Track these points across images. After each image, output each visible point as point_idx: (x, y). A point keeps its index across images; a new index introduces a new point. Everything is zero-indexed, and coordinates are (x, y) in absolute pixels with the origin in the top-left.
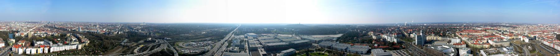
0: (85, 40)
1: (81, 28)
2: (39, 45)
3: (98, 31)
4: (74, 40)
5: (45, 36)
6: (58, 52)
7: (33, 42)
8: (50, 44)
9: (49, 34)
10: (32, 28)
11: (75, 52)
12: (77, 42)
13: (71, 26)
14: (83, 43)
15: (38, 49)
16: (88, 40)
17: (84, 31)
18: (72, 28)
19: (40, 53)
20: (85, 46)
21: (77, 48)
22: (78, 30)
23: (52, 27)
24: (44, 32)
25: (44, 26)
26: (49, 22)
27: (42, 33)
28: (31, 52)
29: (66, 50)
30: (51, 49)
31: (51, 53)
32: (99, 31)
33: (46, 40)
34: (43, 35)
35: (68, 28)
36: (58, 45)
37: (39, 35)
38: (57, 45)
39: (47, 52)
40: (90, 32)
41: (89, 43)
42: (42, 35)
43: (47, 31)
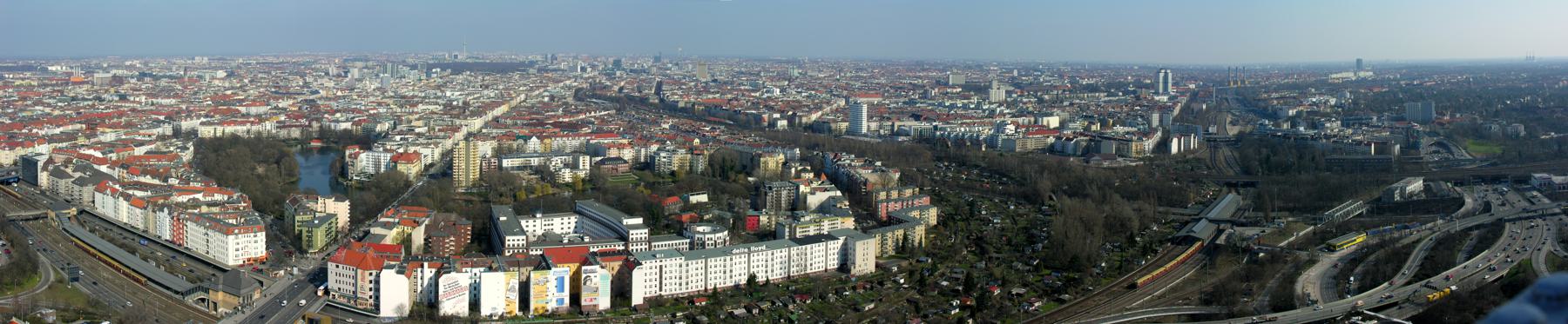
0: (900, 199)
1: (871, 105)
2: (536, 244)
3: (1000, 128)
4: (814, 200)
5: (582, 174)
6: (691, 299)
7: (492, 220)
8: (624, 238)
9: (619, 159)
10: (478, 113)
11: (832, 297)
12: (844, 214)
13: (793, 95)
14: (892, 221)
15: (536, 276)
16: (926, 200)
17: (894, 134)
18: (797, 105)
19: (552, 306)
20: (903, 249)
21: (845, 265)
22: (844, 126)
23: (643, 101)
24: (572, 143)
25: (579, 95)
26: (617, 64)
27: (559, 152)
28: (475, 305)
29: (761, 278)
30: (638, 276)
31: (635, 309)
32: (1010, 129)
33: (593, 207)
34: (566, 165)
35: (771, 109)
36: (692, 246)
37: (535, 162)
38: (683, 243)
39: (604, 302)
40: (943, 140)
41: (933, 221)
42: (557, 162)
43: (598, 132)
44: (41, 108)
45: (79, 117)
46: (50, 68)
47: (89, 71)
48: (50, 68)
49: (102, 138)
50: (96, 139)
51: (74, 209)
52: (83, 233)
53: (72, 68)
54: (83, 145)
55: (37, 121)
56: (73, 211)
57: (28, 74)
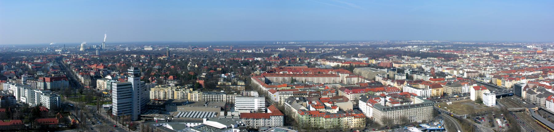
44: (524, 64)
45: (540, 68)
46: (528, 47)
47: (545, 48)
48: (528, 47)
49: (550, 77)
50: (547, 78)
51: (537, 108)
52: (541, 118)
53: (537, 47)
54: (541, 80)
55: (522, 69)
56: (537, 108)
57: (518, 49)
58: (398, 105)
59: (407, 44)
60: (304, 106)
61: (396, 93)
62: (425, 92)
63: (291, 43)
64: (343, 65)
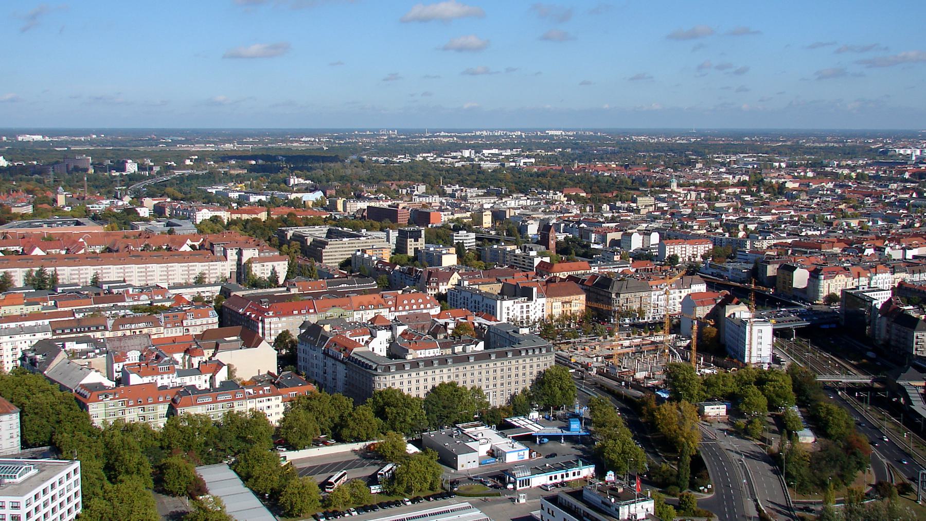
58: (432, 354)
59: (456, 144)
60: (96, 371)
61: (425, 311)
62: (522, 307)
63: (28, 138)
64: (235, 217)
